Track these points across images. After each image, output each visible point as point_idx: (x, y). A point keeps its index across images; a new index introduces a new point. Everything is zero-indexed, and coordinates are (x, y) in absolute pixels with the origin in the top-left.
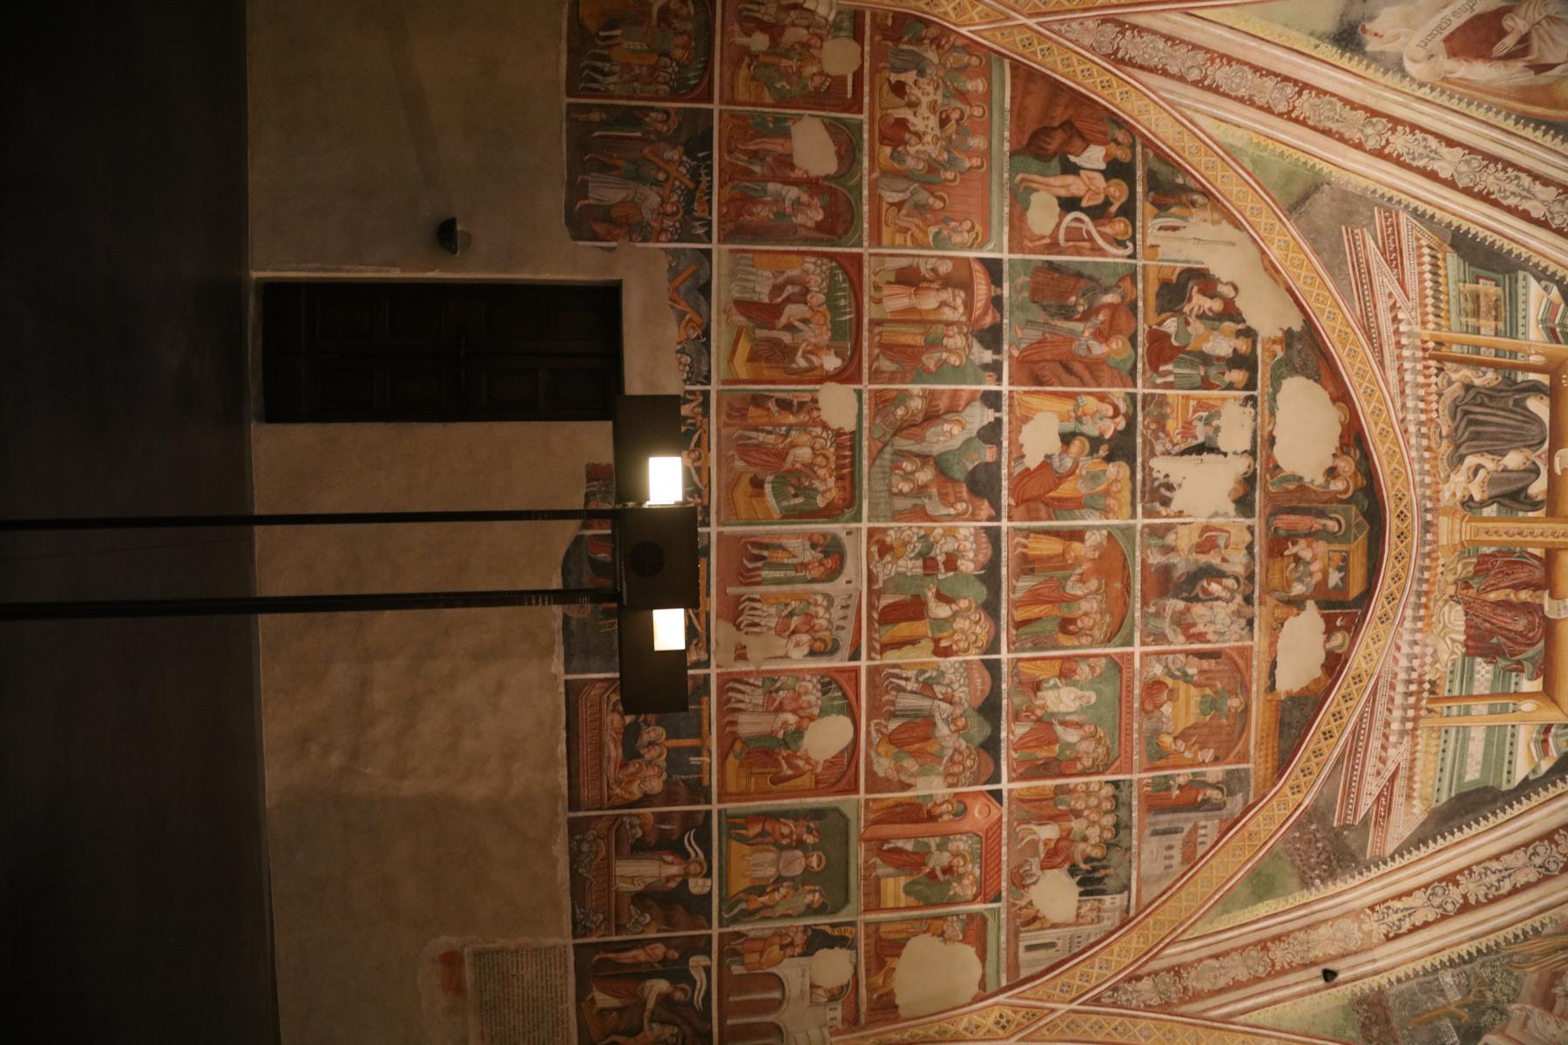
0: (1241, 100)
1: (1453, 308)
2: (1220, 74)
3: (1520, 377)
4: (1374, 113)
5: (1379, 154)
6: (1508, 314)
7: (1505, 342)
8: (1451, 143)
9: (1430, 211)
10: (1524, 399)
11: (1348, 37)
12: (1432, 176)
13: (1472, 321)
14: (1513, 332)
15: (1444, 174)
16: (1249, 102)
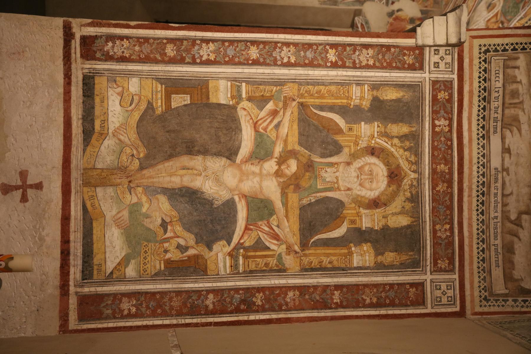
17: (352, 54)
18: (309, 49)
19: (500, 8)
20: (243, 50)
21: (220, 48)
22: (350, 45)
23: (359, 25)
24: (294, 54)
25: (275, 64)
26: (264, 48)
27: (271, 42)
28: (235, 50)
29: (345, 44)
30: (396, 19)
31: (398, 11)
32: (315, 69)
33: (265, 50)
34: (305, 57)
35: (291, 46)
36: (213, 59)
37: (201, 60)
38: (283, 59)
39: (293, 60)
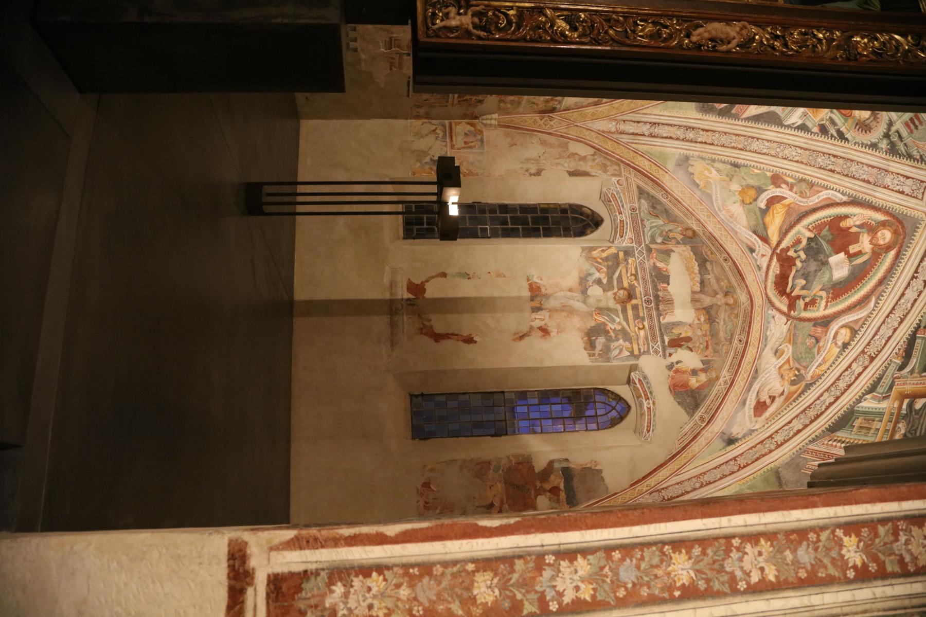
0: (721, 478)
1: (863, 438)
2: (706, 478)
3: (904, 412)
4: (762, 442)
5: (778, 446)
6: (871, 416)
7: (886, 418)
8: (790, 422)
9: (813, 436)
10: (915, 410)
11: (731, 441)
12: (799, 431)
13: (872, 431)
14: (881, 414)
15: (801, 427)
16: (726, 476)
17: (892, 542)
18: (800, 543)
19: (790, 354)
20: (657, 566)
21: (602, 568)
22: (883, 521)
23: (637, 381)
24: (771, 559)
25: (735, 592)
26: (704, 553)
27: (716, 538)
28: (638, 567)
29: (872, 521)
30: (677, 371)
31: (677, 363)
32: (824, 589)
33: (706, 560)
34: (796, 562)
35: (763, 542)
36: (588, 599)
37: (560, 604)
38: (748, 574)
39: (771, 576)
